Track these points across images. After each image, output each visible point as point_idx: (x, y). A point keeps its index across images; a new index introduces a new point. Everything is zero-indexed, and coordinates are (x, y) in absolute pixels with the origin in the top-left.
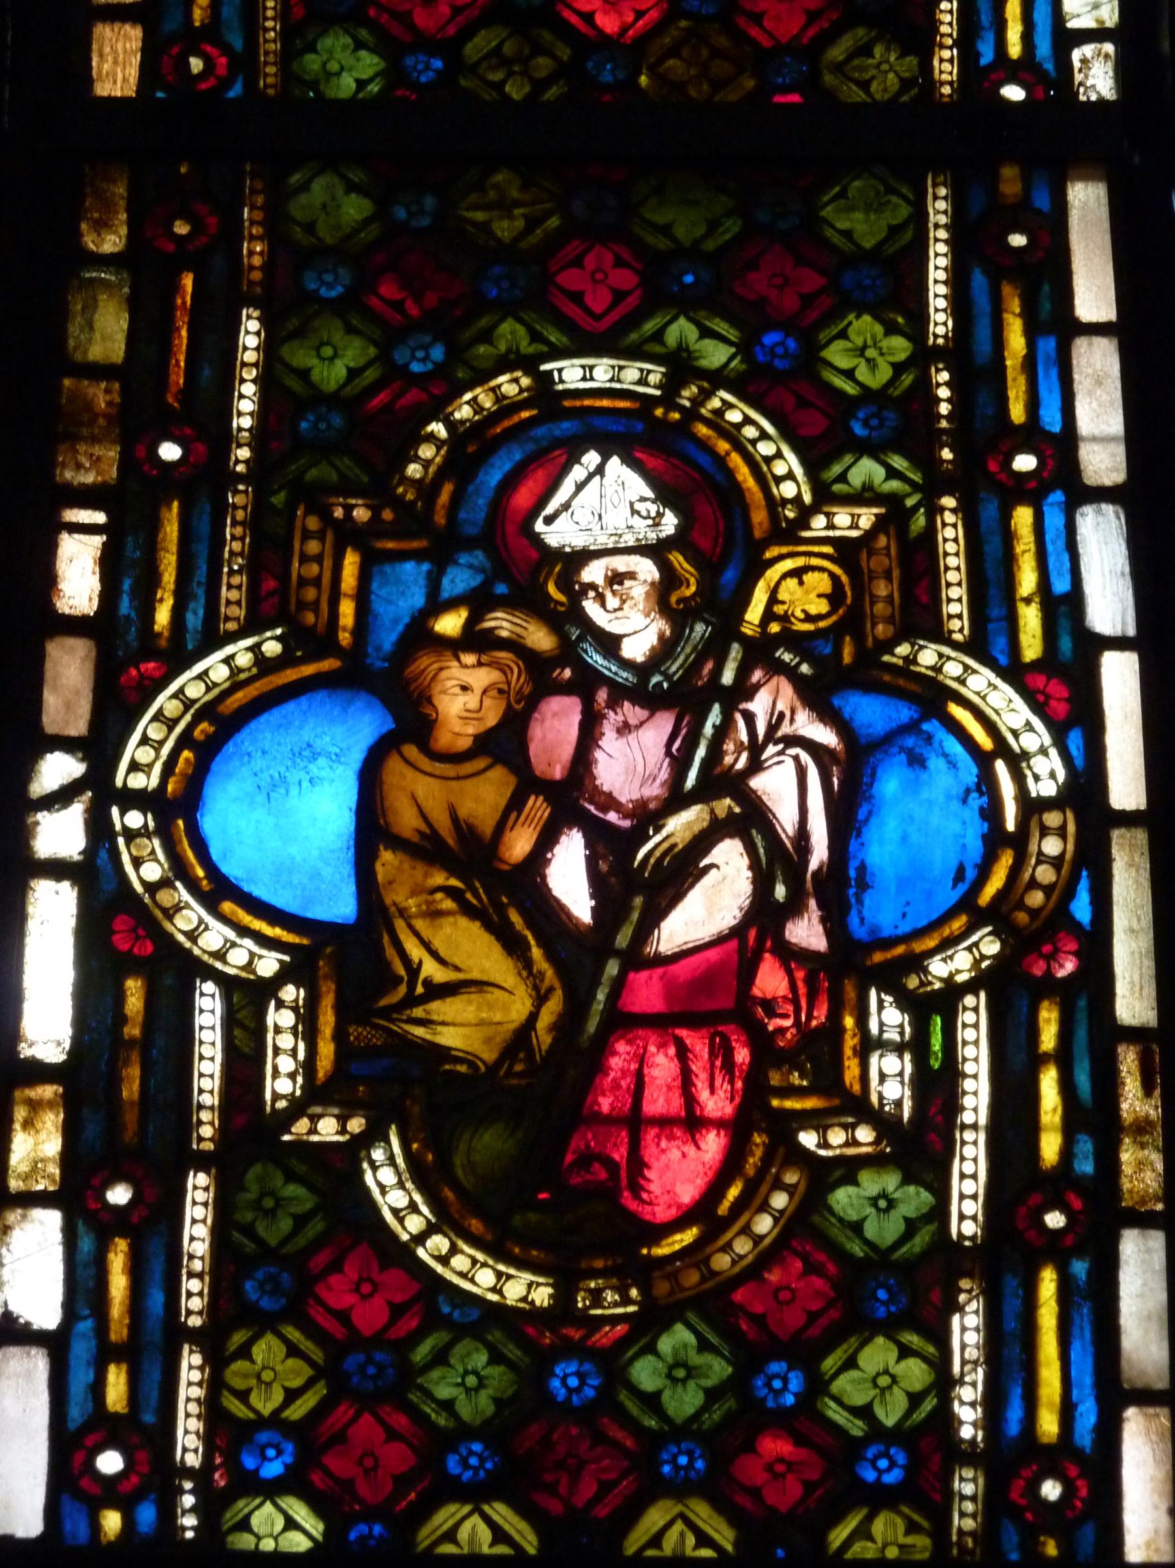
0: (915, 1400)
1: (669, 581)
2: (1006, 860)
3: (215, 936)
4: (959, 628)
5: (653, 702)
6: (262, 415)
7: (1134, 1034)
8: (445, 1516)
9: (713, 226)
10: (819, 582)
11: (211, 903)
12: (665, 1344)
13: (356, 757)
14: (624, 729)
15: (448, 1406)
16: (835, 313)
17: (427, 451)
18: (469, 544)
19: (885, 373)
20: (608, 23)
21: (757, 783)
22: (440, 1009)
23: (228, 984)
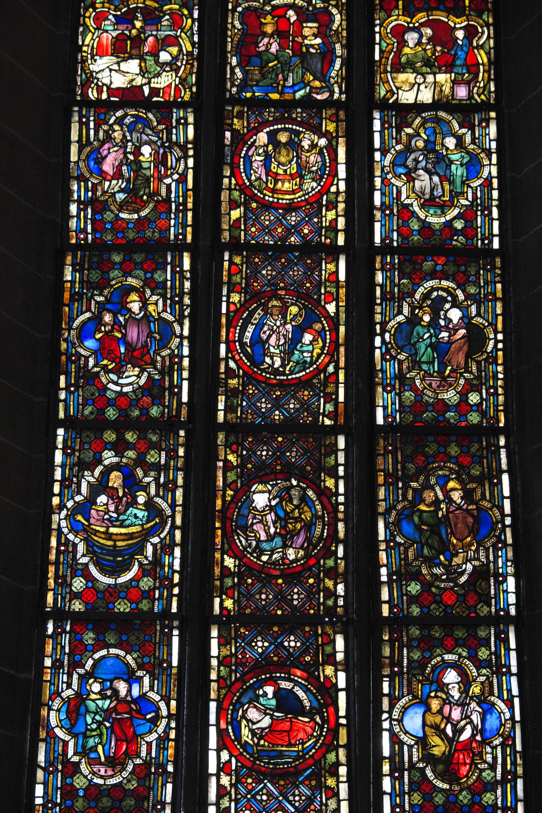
0: (493, 801)
1: (460, 688)
2: (503, 728)
4: (496, 694)
5: (458, 705)
6: (408, 663)
7: (519, 752)
10: (479, 688)
11: (405, 734)
12: (463, 794)
13: (422, 714)
16: (480, 647)
17: (428, 669)
18: (434, 682)
21: (472, 717)
22: (434, 749)
23: (408, 745)
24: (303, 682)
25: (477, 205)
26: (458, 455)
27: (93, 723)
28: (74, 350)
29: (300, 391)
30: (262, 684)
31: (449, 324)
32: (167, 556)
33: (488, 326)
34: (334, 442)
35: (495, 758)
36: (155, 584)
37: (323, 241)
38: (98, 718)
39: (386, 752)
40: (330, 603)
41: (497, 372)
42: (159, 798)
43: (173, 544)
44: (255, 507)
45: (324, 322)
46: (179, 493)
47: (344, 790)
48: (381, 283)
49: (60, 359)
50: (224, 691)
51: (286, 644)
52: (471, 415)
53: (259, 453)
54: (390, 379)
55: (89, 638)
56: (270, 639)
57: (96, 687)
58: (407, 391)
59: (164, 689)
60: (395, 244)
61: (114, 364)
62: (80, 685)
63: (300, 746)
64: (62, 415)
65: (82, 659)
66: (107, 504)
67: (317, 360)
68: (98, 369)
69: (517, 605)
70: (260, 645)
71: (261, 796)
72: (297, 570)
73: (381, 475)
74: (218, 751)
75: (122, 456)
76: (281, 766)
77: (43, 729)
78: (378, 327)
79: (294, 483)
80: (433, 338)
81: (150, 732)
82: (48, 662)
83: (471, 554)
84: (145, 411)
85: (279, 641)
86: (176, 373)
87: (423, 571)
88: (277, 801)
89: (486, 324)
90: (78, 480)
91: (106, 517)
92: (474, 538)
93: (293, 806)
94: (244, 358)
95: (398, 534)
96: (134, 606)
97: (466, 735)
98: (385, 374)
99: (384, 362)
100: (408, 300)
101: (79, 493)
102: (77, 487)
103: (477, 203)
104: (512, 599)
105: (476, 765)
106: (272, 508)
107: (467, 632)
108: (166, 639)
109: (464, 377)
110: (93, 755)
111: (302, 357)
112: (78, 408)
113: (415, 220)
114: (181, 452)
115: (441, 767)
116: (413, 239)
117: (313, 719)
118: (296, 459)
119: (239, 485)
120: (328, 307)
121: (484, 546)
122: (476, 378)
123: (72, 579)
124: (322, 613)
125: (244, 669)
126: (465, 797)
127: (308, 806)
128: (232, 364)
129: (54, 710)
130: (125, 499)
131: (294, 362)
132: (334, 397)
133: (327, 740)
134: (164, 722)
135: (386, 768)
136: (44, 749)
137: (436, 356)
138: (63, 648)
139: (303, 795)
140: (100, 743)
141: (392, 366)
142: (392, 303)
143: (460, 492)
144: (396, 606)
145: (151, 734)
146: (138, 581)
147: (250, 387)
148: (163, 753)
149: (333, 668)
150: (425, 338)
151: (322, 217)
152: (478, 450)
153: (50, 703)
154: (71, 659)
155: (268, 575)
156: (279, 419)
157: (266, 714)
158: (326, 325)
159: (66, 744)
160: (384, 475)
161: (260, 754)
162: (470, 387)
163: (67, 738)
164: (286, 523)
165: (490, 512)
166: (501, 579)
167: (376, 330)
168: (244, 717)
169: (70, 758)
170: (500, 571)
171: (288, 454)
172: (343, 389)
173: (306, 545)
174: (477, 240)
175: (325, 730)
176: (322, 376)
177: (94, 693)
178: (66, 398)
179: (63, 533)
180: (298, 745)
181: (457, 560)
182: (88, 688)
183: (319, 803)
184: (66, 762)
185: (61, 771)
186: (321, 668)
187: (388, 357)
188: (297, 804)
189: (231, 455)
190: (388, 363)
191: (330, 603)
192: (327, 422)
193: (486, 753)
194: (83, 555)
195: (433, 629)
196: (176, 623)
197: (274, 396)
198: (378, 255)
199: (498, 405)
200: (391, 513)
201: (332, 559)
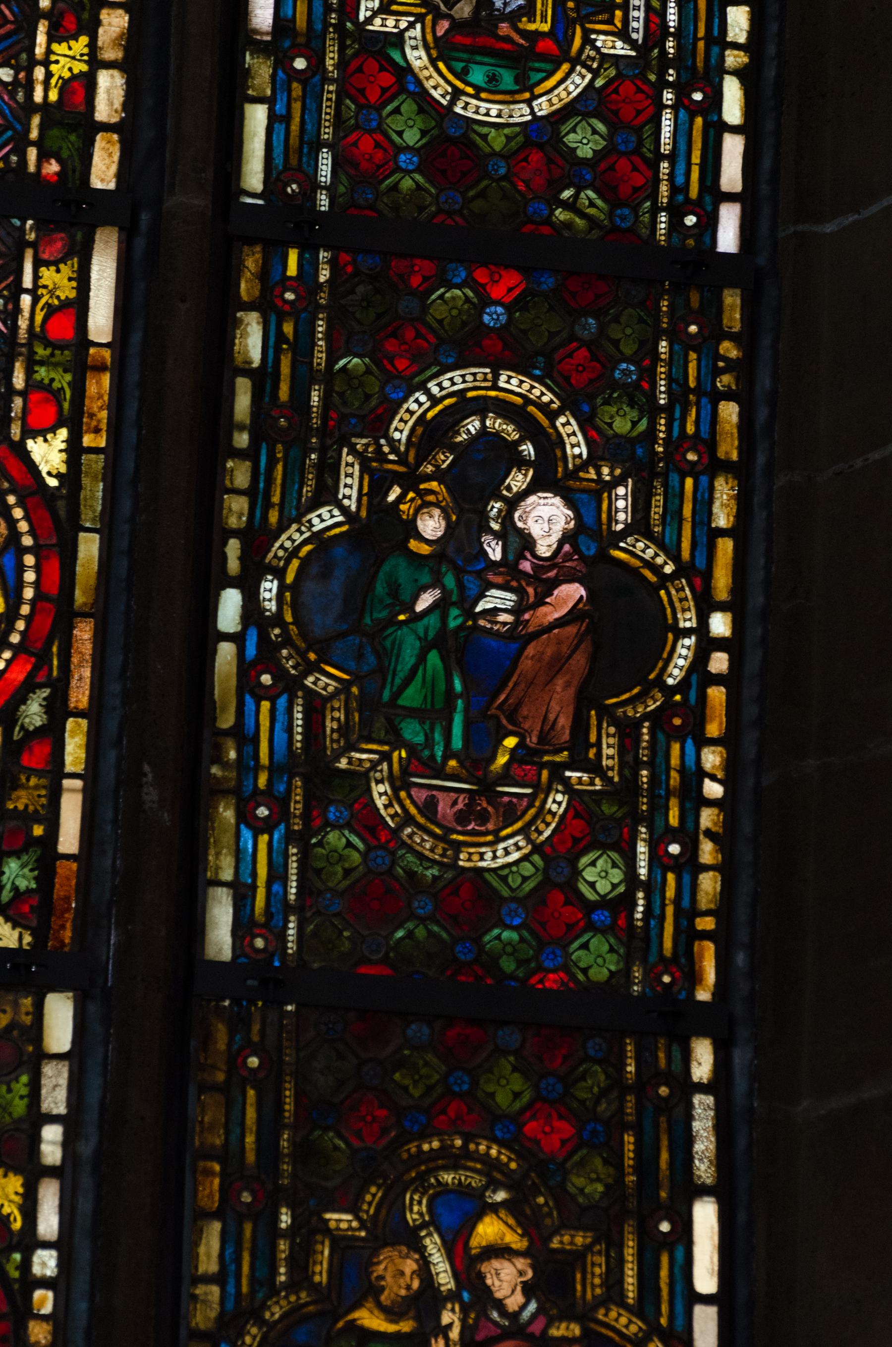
25: (664, 62)
26: (523, 1110)
31: (521, 557)
33: (674, 576)
34: (28, 1020)
37: (32, 168)
41: (702, 774)
45: (18, 513)
48: (256, 363)
52: (585, 946)
54: (274, 769)
58: (334, 827)
60: (323, 202)
73: (210, 1173)
78: (233, 548)
80: (454, 612)
89: (668, 569)
98: (249, 749)
99: (248, 699)
100: (360, 443)
103: (663, 52)
109: (566, 782)
113: (408, 107)
116: (395, 187)
120: (37, 448)
122: (612, 793)
137: (458, 686)
141: (281, 717)
142: (294, 452)
143: (521, 1263)
150: (421, 606)
151: (33, 62)
152: (603, 1093)
158: (23, 526)
160: (223, 1175)
167: (224, 558)
172: (78, 799)
174: (655, 211)
187: (266, 679)
190: (265, 705)
198: (251, 242)
199: (695, 912)
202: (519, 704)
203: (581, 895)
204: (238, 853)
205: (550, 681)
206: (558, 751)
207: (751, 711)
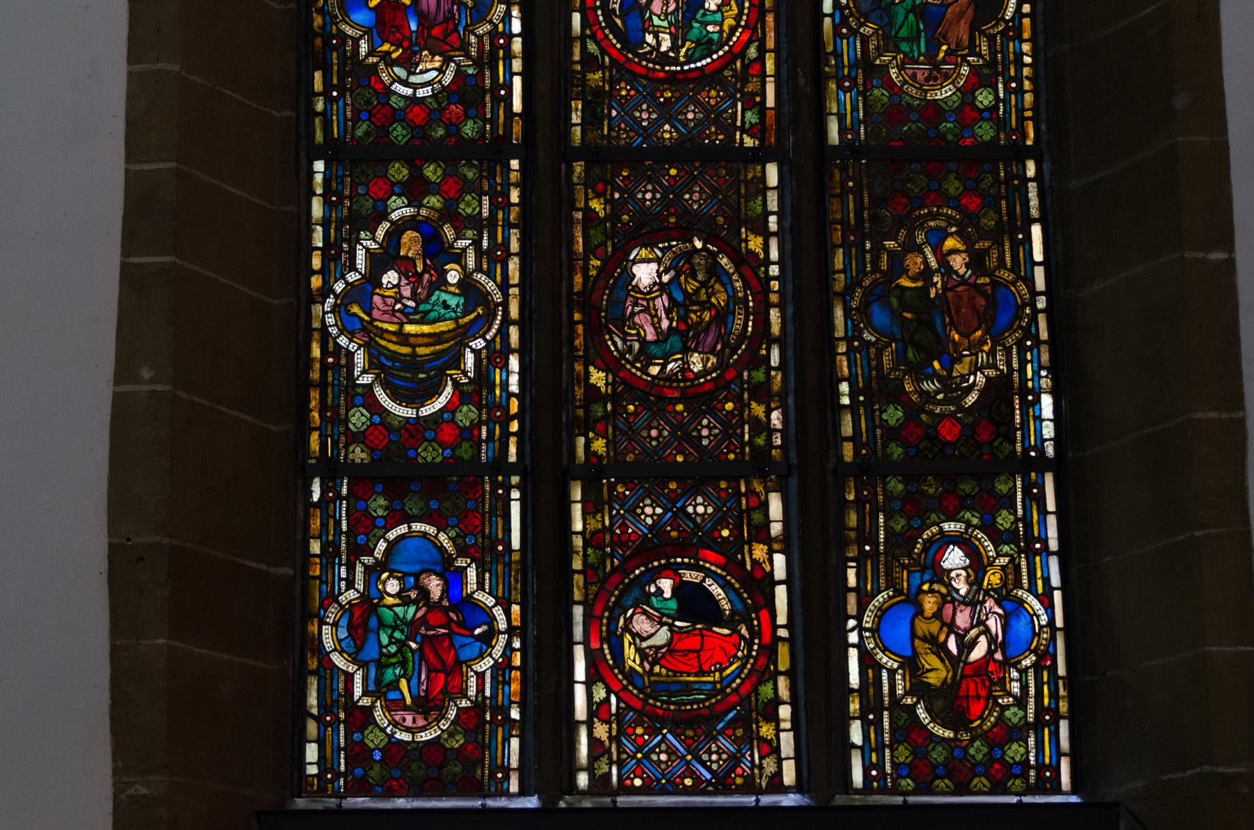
0: (1022, 755)
1: (968, 576)
2: (1036, 639)
3: (885, 659)
4: (1026, 586)
5: (966, 605)
6: (886, 538)
7: (1062, 678)
8: (937, 782)
9: (973, 489)
10: (998, 576)
12: (975, 745)
13: (909, 619)
14: (961, 611)
15: (935, 759)
16: (999, 510)
17: (918, 546)
19: (1009, 524)
20: (949, 438)
21: (988, 622)
22: (929, 674)
24: (719, 571)
26: (960, 195)
27: (390, 643)
28: (334, 27)
29: (704, 90)
30: (654, 575)
32: (498, 371)
34: (760, 175)
35: (1024, 688)
36: (480, 416)
38: (397, 635)
39: (854, 679)
40: (760, 441)
41: (1022, 54)
42: (499, 761)
43: (507, 351)
44: (637, 286)
46: (514, 265)
47: (787, 742)
49: (313, 43)
50: (594, 588)
51: (690, 509)
52: (980, 127)
53: (640, 196)
54: (850, 67)
55: (378, 506)
56: (665, 502)
57: (393, 586)
59: (501, 587)
61: (401, 50)
62: (367, 583)
63: (717, 674)
64: (319, 137)
65: (368, 540)
66: (398, 286)
67: (729, 38)
68: (375, 60)
69: (1057, 440)
70: (650, 512)
71: (658, 754)
72: (707, 388)
73: (836, 230)
74: (589, 684)
75: (420, 206)
76: (689, 707)
77: (313, 655)
79: (699, 244)
81: (481, 656)
82: (315, 547)
83: (982, 358)
84: (453, 128)
85: (679, 505)
86: (501, 63)
87: (907, 386)
88: (683, 763)
90: (350, 247)
91: (398, 306)
92: (986, 332)
93: (709, 769)
94: (611, 36)
95: (865, 327)
96: (448, 452)
97: (979, 652)
98: (840, 59)
99: (838, 39)
101: (353, 268)
102: (349, 258)
104: (1048, 430)
105: (995, 698)
106: (662, 287)
107: (978, 485)
108: (499, 505)
109: (968, 62)
110: (393, 695)
111: (704, 32)
112: (345, 125)
114: (515, 196)
115: (939, 704)
117: (735, 631)
118: (700, 205)
119: (610, 249)
121: (1003, 345)
122: (986, 65)
123: (347, 411)
124: (747, 458)
125: (625, 552)
126: (978, 751)
127: (733, 769)
128: (592, 47)
129: (328, 624)
130: (427, 276)
131: (692, 42)
132: (758, 99)
133: (760, 663)
134: (503, 639)
135: (854, 706)
136: (315, 686)
137: (922, 27)
138: (338, 523)
139: (724, 752)
140: (403, 676)
141: (851, 45)
143: (964, 255)
144: (864, 445)
145: (484, 659)
146: (453, 413)
147: (623, 85)
148: (503, 689)
149: (766, 547)
152: (992, 185)
153: (322, 612)
154: (352, 540)
155: (660, 398)
156: (670, 139)
157: (662, 624)
159: (349, 678)
160: (842, 230)
161: (656, 688)
162: (980, 79)
163: (351, 668)
164: (688, 311)
165: (1013, 289)
166: (1030, 398)
168: (627, 628)
169: (358, 701)
170: (1030, 384)
171: (687, 196)
172: (773, 85)
173: (719, 347)
175: (756, 647)
176: (738, 64)
177: (389, 595)
178: (325, 109)
179: (330, 334)
180: (714, 672)
181: (960, 369)
182: (380, 587)
183: (748, 764)
184: (351, 707)
185: (344, 722)
186: (746, 547)
187: (844, 31)
188: (715, 767)
189: (595, 201)
190: (845, 41)
191: (760, 441)
192: (749, 142)
193: (1011, 680)
194: (364, 372)
195: (925, 481)
196: (515, 480)
197: (662, 100)
199: (1024, 110)
200: (854, 292)
201: (762, 370)
202: (946, 33)
203: (977, 107)
204: (838, 101)
205: (959, 21)
206: (963, 50)
207: (1041, 27)
